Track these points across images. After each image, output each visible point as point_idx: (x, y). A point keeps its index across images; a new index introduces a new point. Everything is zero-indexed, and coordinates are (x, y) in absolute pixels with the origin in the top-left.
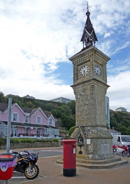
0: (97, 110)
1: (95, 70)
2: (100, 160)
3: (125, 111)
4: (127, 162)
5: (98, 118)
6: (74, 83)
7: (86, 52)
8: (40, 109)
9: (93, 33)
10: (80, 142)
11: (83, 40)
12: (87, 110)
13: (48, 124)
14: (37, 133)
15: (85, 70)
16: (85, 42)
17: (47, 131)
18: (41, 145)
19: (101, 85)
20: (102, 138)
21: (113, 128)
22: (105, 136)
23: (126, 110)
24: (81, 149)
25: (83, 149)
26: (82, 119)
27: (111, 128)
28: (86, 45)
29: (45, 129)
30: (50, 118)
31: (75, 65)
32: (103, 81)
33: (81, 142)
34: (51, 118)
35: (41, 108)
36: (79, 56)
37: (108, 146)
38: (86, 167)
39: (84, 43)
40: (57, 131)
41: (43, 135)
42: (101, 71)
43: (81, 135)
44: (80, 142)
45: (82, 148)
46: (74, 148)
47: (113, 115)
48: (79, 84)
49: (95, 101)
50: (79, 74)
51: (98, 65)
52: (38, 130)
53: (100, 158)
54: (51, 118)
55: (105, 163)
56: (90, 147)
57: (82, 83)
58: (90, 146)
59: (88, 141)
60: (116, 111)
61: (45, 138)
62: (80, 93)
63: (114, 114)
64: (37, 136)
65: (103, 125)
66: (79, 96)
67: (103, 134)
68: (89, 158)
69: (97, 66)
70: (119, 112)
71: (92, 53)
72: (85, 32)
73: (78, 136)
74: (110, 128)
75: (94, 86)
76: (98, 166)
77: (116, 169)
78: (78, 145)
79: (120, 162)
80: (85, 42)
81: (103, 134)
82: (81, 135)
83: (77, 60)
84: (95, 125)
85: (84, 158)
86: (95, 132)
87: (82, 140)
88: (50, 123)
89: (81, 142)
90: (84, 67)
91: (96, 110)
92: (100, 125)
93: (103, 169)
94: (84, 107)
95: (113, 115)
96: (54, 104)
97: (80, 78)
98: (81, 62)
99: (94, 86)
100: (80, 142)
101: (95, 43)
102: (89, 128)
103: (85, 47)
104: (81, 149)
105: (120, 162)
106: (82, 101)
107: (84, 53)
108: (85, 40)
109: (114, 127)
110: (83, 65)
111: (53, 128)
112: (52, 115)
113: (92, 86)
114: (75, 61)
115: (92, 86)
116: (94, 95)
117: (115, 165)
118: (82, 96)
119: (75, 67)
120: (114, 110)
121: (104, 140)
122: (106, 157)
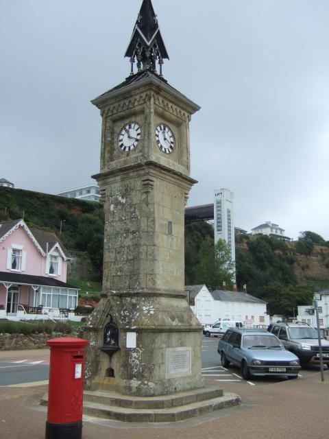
0: (158, 250)
1: (158, 136)
2: (159, 395)
3: (279, 233)
4: (238, 401)
5: (161, 272)
6: (102, 169)
7: (135, 89)
8: (22, 223)
9: (155, 37)
10: (110, 342)
11: (132, 53)
12: (132, 248)
13: (46, 273)
14: (9, 300)
15: (129, 138)
16: (136, 58)
17: (39, 294)
18: (16, 343)
19: (173, 179)
20: (171, 331)
21: (245, 287)
22: (180, 324)
23: (282, 230)
24: (110, 361)
25: (116, 364)
26: (119, 274)
27: (240, 288)
28: (139, 65)
29: (35, 289)
30: (52, 252)
31: (108, 120)
32: (179, 168)
33: (113, 342)
34: (56, 254)
35: (26, 221)
36: (116, 97)
37: (188, 353)
38: (119, 416)
39: (132, 61)
40: (71, 299)
41: (28, 309)
42: (174, 139)
43: (111, 319)
44: (109, 339)
45: (115, 359)
46: (79, 362)
47: (245, 246)
48: (112, 173)
49: (154, 224)
50: (116, 145)
51: (167, 123)
52: (12, 292)
53: (159, 389)
54: (56, 254)
55: (172, 404)
57: (123, 171)
59: (131, 340)
60: (254, 233)
61: (32, 317)
62: (117, 199)
63: (247, 243)
64: (8, 311)
65: (175, 291)
66: (112, 206)
67: (173, 319)
68: (130, 388)
69: (162, 127)
70: (265, 238)
71: (148, 92)
72: (136, 35)
73: (105, 324)
74: (235, 286)
75: (151, 183)
76: (149, 415)
77: (198, 421)
78: (104, 351)
79: (221, 400)
80: (136, 58)
81: (173, 319)
82: (111, 319)
83: (112, 107)
84: (150, 291)
85: (116, 389)
86: (149, 313)
87: (115, 336)
88: (52, 271)
89: (113, 342)
90: (130, 126)
91: (156, 248)
92: (165, 292)
93: (163, 423)
94: (126, 238)
95: (245, 245)
96: (70, 207)
97: (119, 157)
98: (122, 113)
99: (151, 183)
100: (109, 339)
101: (161, 63)
102: (134, 301)
103: (136, 71)
104: (110, 361)
105: (221, 400)
106: (121, 220)
107: (129, 92)
108: (137, 54)
109: (247, 283)
110: (127, 121)
111: (59, 284)
112: (57, 245)
113: (145, 182)
114: (106, 110)
115: (145, 182)
116: (150, 206)
117: (194, 411)
118: (120, 207)
119: (108, 125)
120: (249, 232)
122: (180, 388)
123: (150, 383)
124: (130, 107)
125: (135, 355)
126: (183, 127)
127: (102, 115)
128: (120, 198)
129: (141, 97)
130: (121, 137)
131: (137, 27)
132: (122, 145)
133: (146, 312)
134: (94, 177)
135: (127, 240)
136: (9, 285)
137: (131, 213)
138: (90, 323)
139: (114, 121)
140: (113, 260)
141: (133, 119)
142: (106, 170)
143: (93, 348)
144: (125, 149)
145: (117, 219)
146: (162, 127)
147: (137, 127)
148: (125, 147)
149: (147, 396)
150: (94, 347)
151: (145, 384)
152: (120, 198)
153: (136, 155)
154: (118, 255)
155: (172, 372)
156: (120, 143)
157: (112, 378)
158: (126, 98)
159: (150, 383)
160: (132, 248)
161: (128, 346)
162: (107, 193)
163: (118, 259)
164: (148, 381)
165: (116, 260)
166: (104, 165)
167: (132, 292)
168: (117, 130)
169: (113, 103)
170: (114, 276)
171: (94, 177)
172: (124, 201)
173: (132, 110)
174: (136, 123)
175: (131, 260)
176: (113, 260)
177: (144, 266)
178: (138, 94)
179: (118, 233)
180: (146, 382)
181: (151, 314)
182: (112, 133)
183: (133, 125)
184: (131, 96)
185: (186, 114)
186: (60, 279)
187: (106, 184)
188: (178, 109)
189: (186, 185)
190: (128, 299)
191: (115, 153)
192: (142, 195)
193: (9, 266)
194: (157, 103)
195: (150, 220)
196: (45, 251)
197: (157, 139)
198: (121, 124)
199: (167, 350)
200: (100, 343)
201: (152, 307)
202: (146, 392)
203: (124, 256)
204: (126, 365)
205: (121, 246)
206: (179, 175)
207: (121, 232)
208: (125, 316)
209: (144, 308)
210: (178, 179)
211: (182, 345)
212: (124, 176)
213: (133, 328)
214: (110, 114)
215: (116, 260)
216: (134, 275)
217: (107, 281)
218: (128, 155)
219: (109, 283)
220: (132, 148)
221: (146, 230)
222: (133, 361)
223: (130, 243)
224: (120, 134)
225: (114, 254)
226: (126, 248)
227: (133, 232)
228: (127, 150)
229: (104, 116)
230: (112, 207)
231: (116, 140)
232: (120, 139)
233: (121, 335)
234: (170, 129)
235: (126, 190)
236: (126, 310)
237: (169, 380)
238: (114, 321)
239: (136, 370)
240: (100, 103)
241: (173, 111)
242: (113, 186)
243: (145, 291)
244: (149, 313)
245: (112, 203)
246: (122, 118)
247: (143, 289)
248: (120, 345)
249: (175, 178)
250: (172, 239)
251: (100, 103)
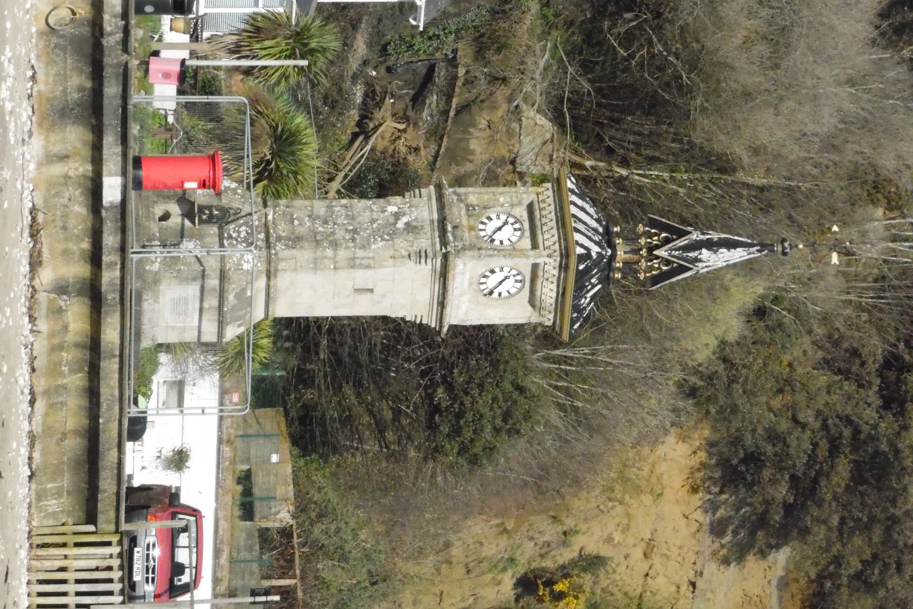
62: (404, 214)
118: (392, 220)
128: (405, 219)
135: (342, 233)
144: (483, 223)
152: (405, 219)
172: (400, 225)
177: (304, 255)
179: (353, 218)
192: (407, 251)
207: (355, 224)
208: (239, 232)
216: (295, 241)
228: (481, 227)
230: (392, 209)
232: (501, 216)
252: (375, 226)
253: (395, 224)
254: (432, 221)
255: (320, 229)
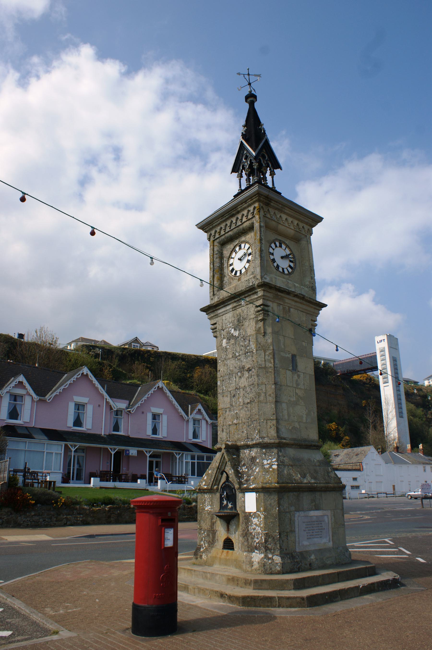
5: (286, 417)
10: (227, 505)
16: (244, 173)
22: (313, 481)
26: (235, 422)
28: (248, 180)
31: (216, 243)
32: (305, 291)
33: (230, 506)
44: (225, 502)
48: (223, 303)
56: (256, 524)
58: (255, 521)
62: (229, 333)
65: (305, 440)
83: (219, 228)
87: (232, 498)
89: (230, 506)
90: (240, 246)
92: (292, 442)
94: (240, 377)
98: (230, 233)
100: (225, 502)
101: (272, 174)
106: (234, 357)
110: (237, 242)
118: (232, 341)
121: (306, 498)
123: (275, 557)
124: (238, 224)
125: (255, 521)
126: (304, 243)
127: (209, 239)
129: (249, 211)
130: (231, 261)
131: (242, 139)
132: (233, 269)
133: (267, 466)
134: (203, 310)
135: (243, 380)
136: (150, 452)
137: (246, 347)
138: (204, 483)
139: (223, 244)
140: (229, 406)
141: (243, 239)
142: (216, 299)
143: (208, 514)
145: (231, 356)
146: (278, 244)
147: (247, 246)
148: (236, 272)
149: (271, 574)
150: (209, 513)
151: (269, 559)
153: (248, 278)
154: (233, 399)
155: (306, 543)
156: (231, 268)
157: (230, 551)
158: (233, 216)
159: (275, 557)
160: (248, 389)
161: (247, 510)
162: (219, 327)
163: (234, 404)
164: (273, 554)
165: (232, 405)
166: (214, 295)
167: (250, 443)
168: (226, 253)
169: (219, 224)
170: (230, 425)
171: (203, 310)
172: (236, 334)
173: (241, 227)
174: (246, 242)
175: (248, 403)
176: (229, 406)
178: (245, 208)
180: (270, 556)
181: (274, 469)
182: (221, 257)
183: (243, 245)
184: (238, 212)
185: (306, 227)
186: (204, 445)
187: (217, 316)
188: (296, 222)
189: (313, 310)
190: (247, 451)
191: (226, 279)
193: (149, 431)
194: (268, 216)
195: (267, 353)
196: (187, 414)
197: (272, 257)
198: (230, 247)
199: (297, 514)
200: (217, 508)
201: (274, 460)
202: (271, 569)
203: (241, 400)
204: (246, 534)
205: (236, 388)
206: (302, 298)
209: (265, 462)
210: (301, 303)
211: (317, 508)
212: (235, 304)
213: (251, 487)
214: (217, 236)
215: (232, 405)
217: (223, 431)
218: (239, 280)
219: (224, 434)
220: (243, 271)
221: (263, 366)
222: (254, 529)
223: (246, 384)
224: (230, 257)
225: (229, 398)
226: (241, 390)
227: (249, 370)
228: (238, 274)
229: (212, 239)
231: (225, 265)
232: (231, 263)
233: (239, 495)
234: (287, 246)
235: (239, 320)
236: (244, 465)
237: (301, 553)
238: (230, 479)
239: (257, 541)
240: (206, 226)
241: (287, 224)
242: (224, 317)
243: (266, 440)
244: (271, 467)
245: (224, 338)
246: (231, 239)
247: (263, 438)
248: (238, 508)
249: (296, 302)
250: (299, 376)
251: (206, 226)
252: (237, 354)
253: (236, 338)
254: (234, 308)
255: (241, 400)
